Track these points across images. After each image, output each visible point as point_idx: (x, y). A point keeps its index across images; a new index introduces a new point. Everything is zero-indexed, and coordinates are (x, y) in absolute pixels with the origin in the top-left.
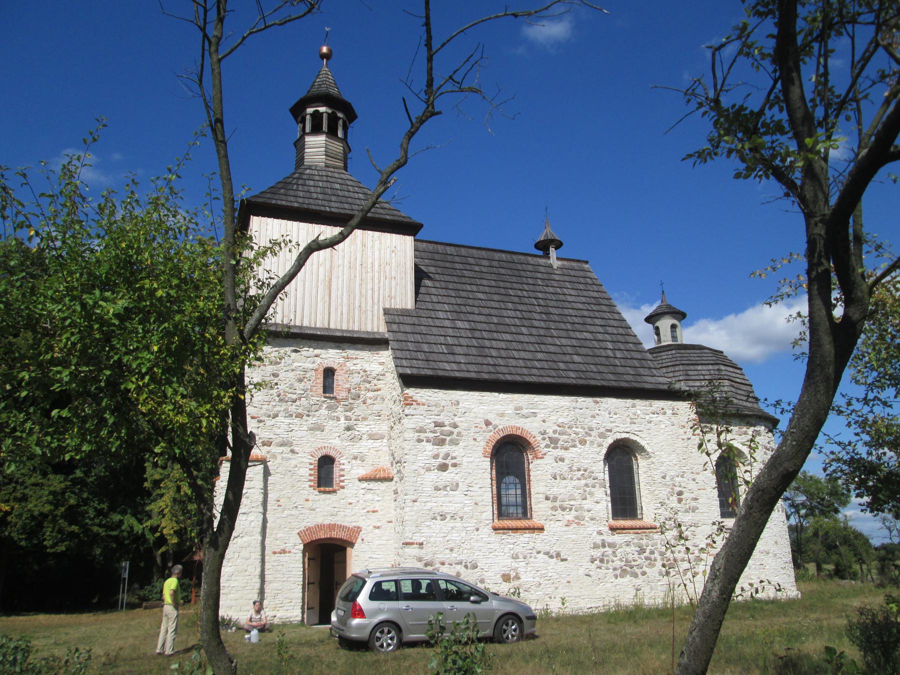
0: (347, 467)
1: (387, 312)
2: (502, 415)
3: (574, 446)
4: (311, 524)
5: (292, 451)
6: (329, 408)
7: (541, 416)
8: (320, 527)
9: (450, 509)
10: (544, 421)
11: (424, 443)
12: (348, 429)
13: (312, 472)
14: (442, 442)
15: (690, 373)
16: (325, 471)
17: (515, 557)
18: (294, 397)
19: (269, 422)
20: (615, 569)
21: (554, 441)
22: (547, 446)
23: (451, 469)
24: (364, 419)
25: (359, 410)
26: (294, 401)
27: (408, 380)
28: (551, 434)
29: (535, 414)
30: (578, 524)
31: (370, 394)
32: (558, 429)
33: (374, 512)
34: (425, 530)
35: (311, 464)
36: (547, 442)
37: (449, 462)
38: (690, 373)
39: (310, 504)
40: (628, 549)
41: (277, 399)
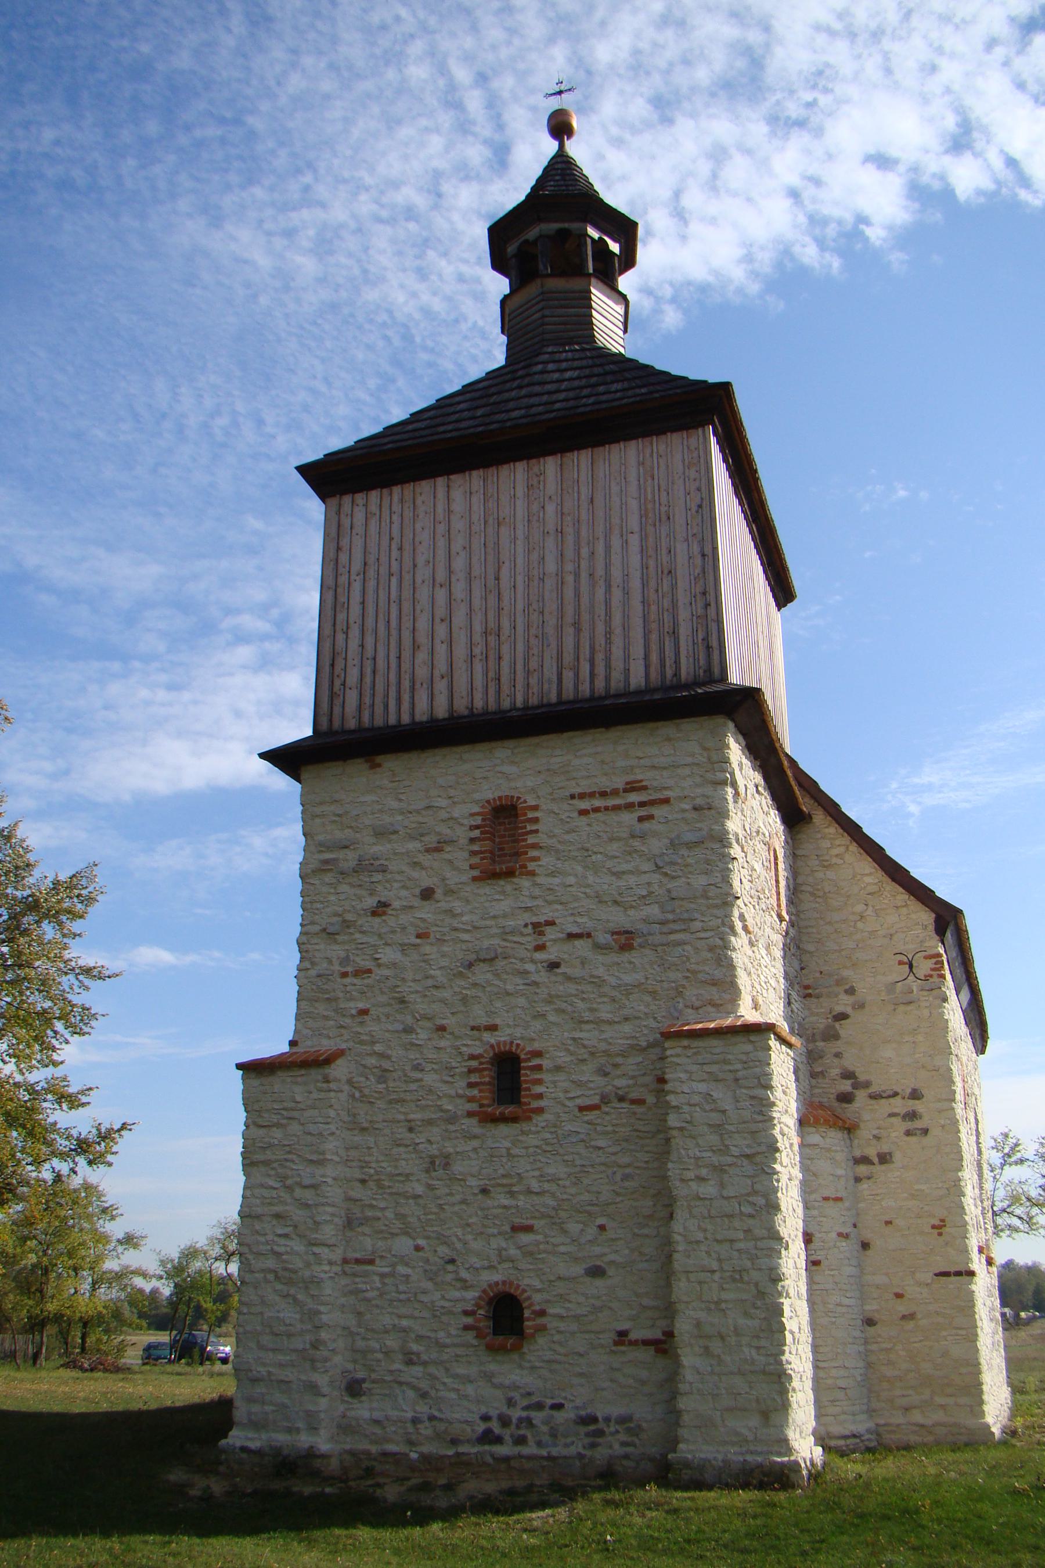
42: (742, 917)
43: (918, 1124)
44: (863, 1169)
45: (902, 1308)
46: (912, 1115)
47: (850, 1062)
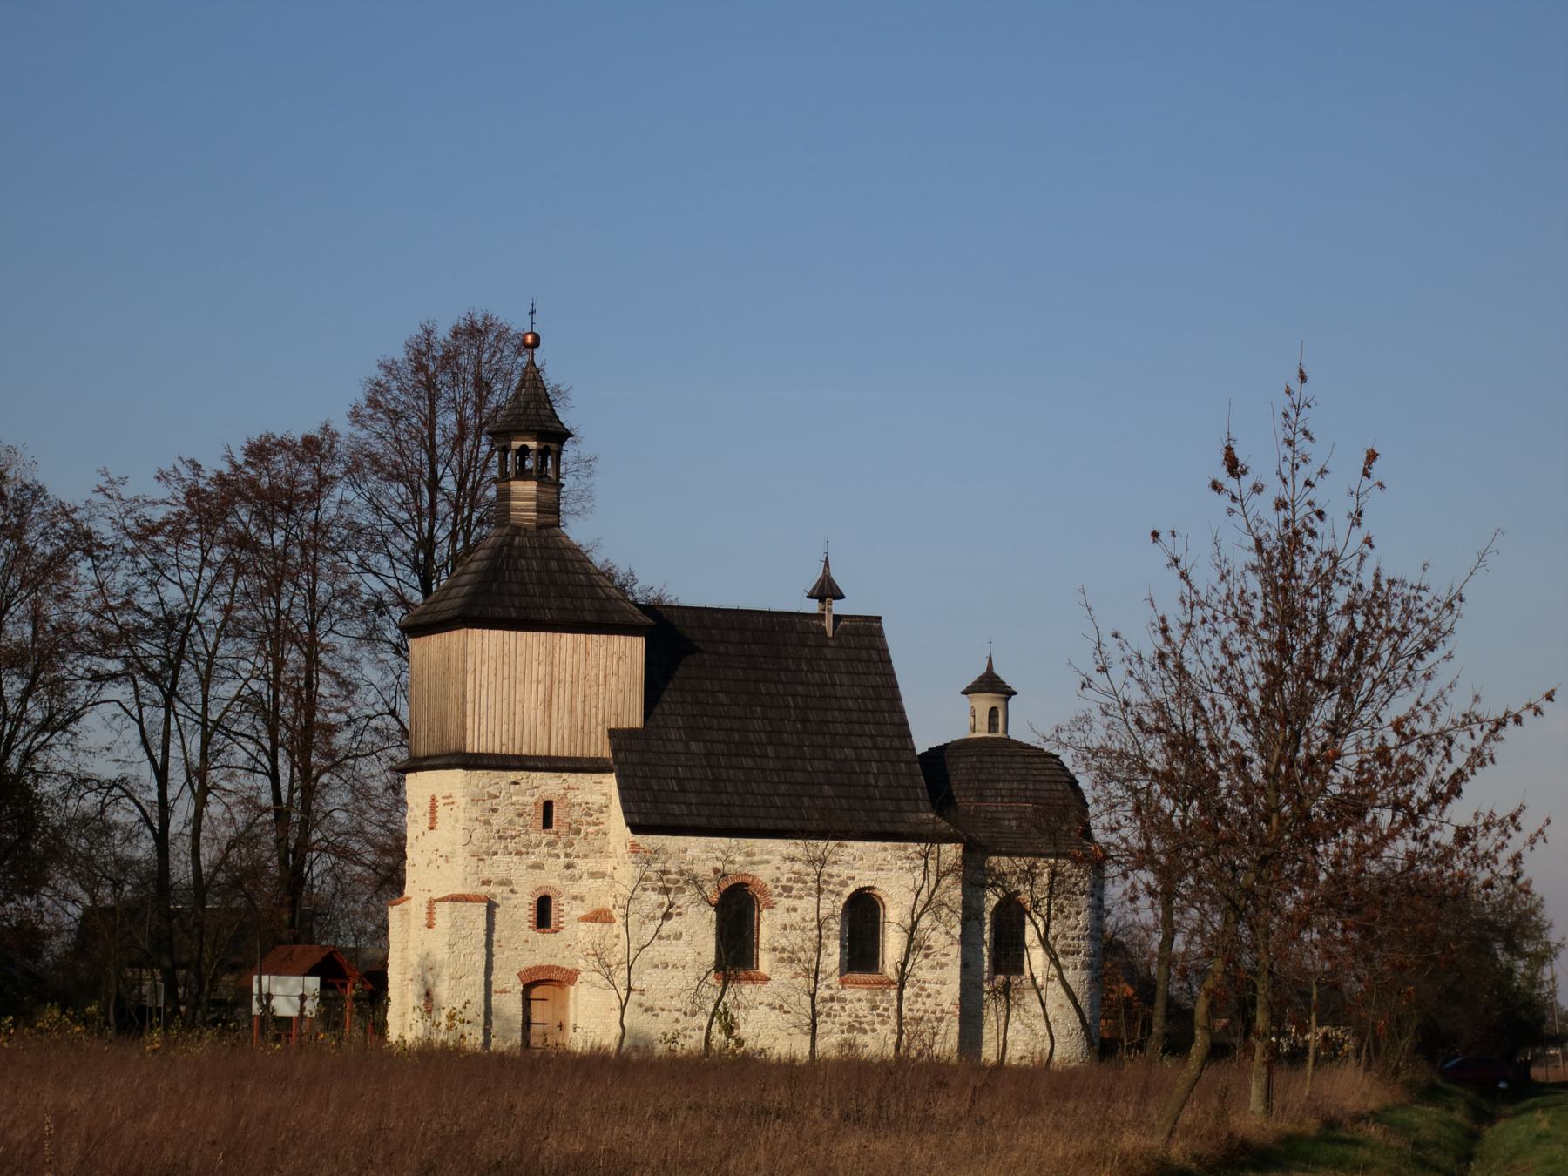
0: (566, 908)
1: (612, 733)
5: (512, 891)
6: (549, 844)
8: (540, 968)
12: (568, 867)
16: (543, 913)
19: (489, 861)
22: (780, 895)
23: (675, 919)
24: (586, 856)
25: (579, 846)
26: (513, 837)
27: (636, 828)
28: (784, 883)
29: (768, 862)
31: (591, 829)
36: (779, 890)
40: (858, 1005)
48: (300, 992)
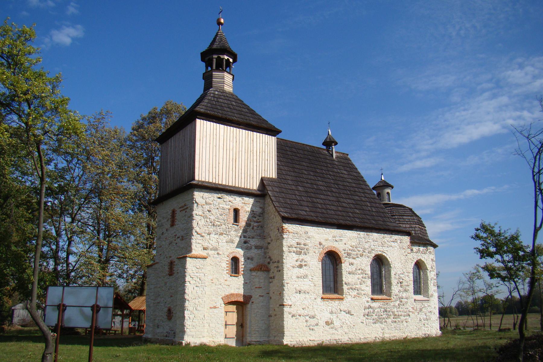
2: (327, 240)
3: (358, 257)
4: (227, 294)
5: (218, 254)
7: (344, 241)
8: (232, 295)
9: (304, 288)
10: (345, 244)
11: (292, 253)
13: (228, 265)
14: (300, 253)
15: (401, 220)
17: (332, 313)
18: (219, 223)
20: (373, 319)
21: (349, 254)
22: (346, 257)
24: (253, 238)
30: (359, 297)
32: (351, 248)
33: (259, 288)
34: (292, 298)
35: (227, 261)
37: (303, 263)
38: (401, 220)
39: (227, 283)
41: (210, 224)
42: (196, 232)
43: (279, 269)
44: (271, 280)
45: (275, 313)
46: (278, 267)
47: (270, 254)
48: (92, 302)
